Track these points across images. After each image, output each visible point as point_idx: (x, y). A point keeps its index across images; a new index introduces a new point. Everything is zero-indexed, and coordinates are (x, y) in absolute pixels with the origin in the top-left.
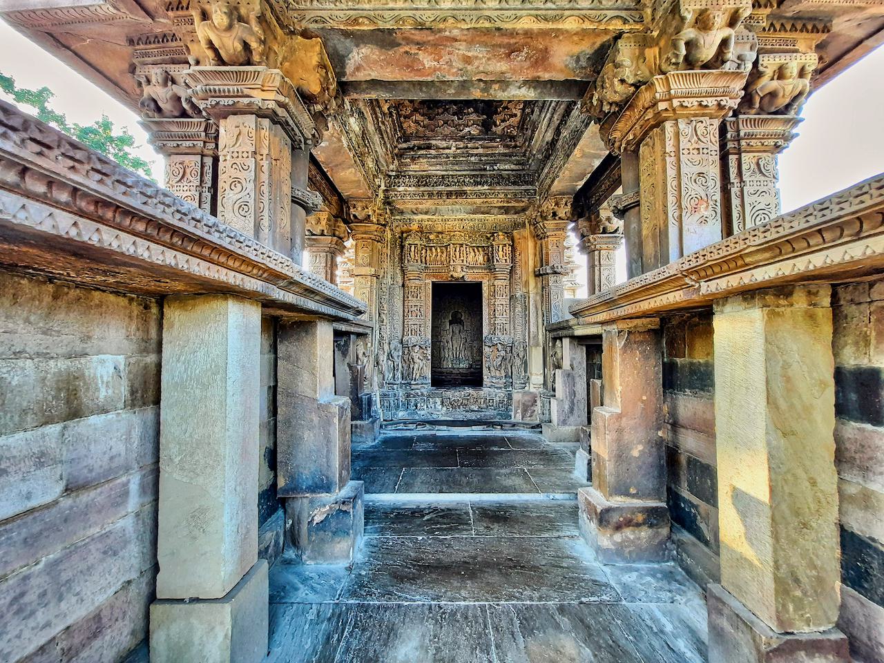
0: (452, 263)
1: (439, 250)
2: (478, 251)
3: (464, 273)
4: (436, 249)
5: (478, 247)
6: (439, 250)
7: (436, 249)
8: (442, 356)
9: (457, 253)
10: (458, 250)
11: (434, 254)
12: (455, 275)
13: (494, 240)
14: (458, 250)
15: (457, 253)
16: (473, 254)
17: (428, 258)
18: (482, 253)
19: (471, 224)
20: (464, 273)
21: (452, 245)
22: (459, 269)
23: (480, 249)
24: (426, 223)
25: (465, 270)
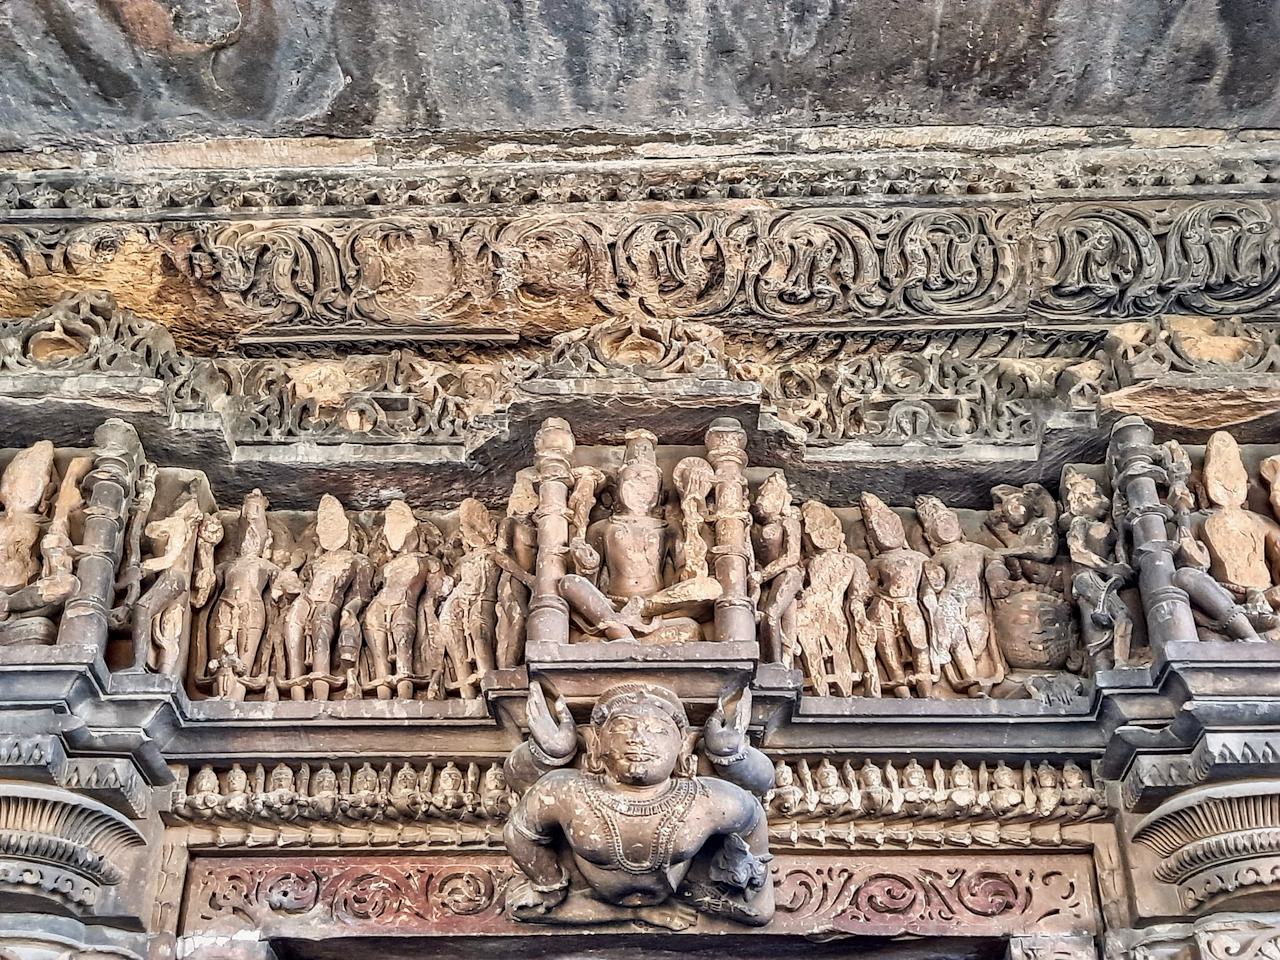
0: (551, 642)
1: (399, 524)
2: (925, 539)
3: (727, 802)
4: (367, 533)
5: (911, 486)
6: (399, 524)
7: (367, 533)
9: (636, 536)
10: (638, 492)
11: (331, 570)
12: (599, 813)
13: (1113, 380)
14: (638, 492)
15: (636, 536)
16: (838, 568)
17: (239, 619)
18: (966, 556)
19: (809, 228)
20: (727, 802)
21: (556, 438)
22: (653, 732)
23: (936, 511)
24: (261, 227)
25: (733, 730)
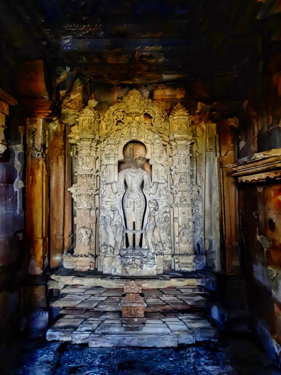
8: (102, 240)
